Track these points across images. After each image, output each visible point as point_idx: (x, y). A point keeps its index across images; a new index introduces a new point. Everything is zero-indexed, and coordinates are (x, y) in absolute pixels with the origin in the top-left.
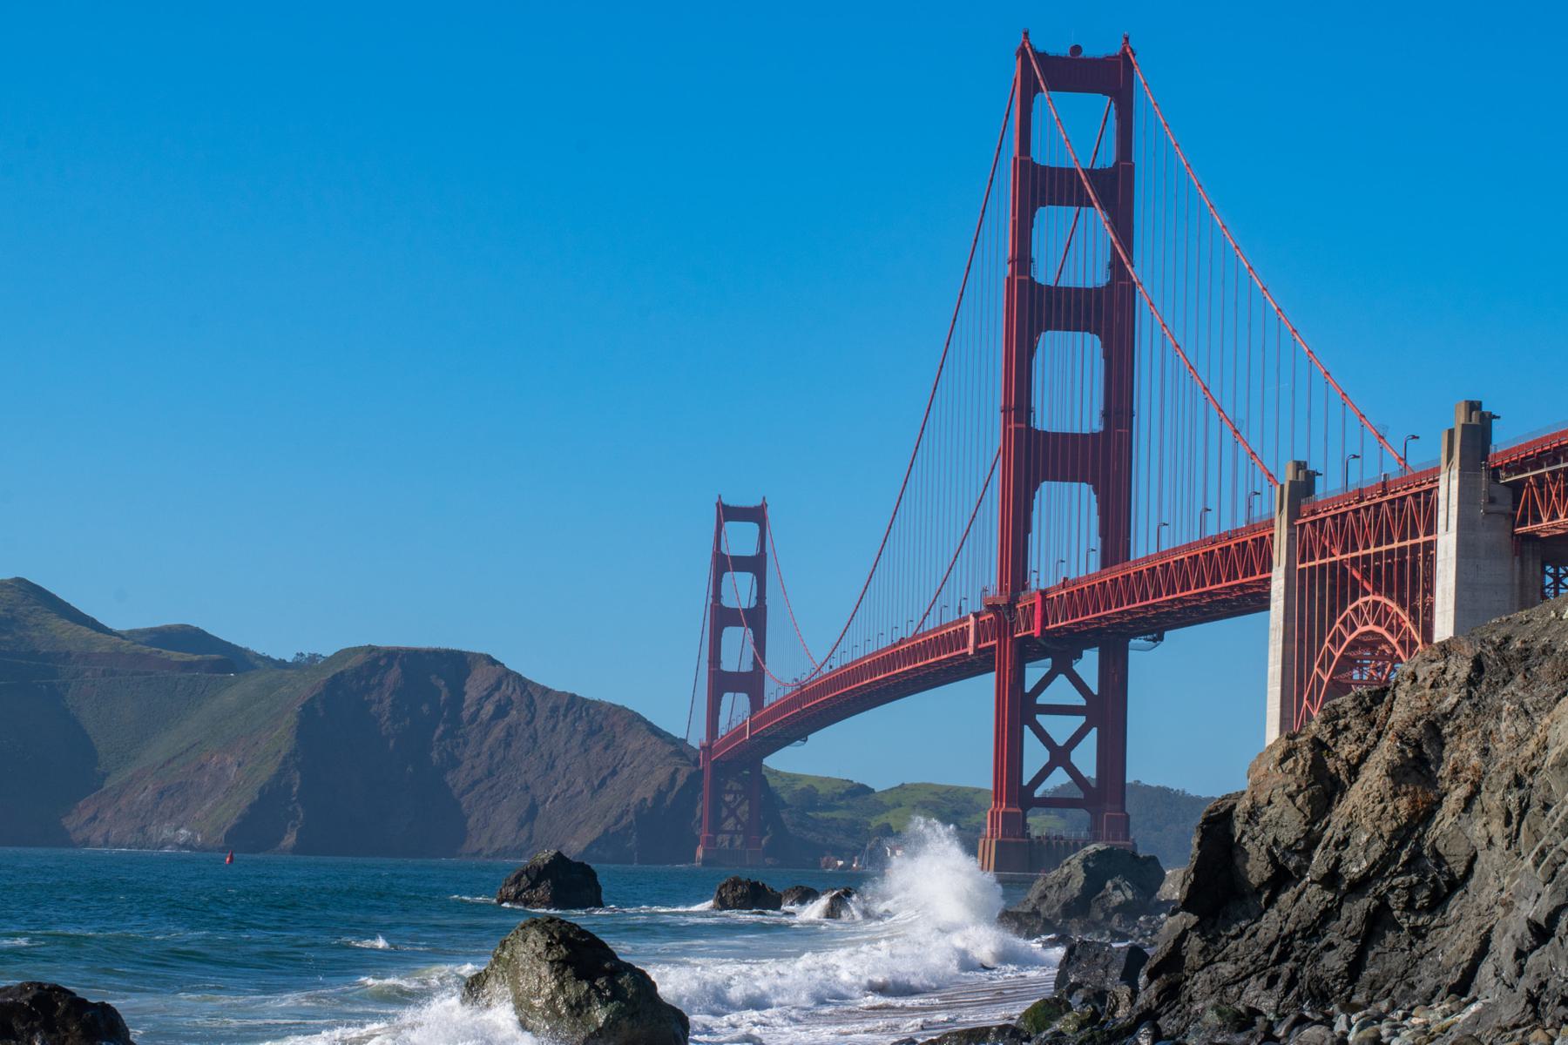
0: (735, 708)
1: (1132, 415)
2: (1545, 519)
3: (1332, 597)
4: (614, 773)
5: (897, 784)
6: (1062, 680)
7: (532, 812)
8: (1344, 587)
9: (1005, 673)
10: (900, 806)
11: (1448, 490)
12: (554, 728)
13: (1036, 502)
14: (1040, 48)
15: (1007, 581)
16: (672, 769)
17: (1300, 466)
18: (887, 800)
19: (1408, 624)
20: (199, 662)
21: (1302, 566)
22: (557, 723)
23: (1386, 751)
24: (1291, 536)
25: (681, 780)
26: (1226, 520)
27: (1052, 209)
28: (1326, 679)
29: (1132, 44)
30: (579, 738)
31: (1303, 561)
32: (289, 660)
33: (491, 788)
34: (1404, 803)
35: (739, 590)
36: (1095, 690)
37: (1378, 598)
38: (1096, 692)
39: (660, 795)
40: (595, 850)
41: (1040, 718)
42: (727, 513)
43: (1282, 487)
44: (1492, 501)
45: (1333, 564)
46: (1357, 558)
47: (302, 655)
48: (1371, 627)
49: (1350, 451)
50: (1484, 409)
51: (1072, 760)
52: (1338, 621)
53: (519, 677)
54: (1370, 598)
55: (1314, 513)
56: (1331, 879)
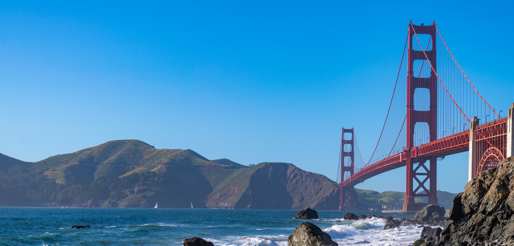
0: (347, 175)
1: (437, 107)
3: (483, 147)
4: (321, 190)
6: (421, 167)
7: (302, 199)
8: (486, 145)
9: (408, 166)
10: (385, 196)
12: (307, 180)
13: (415, 127)
14: (414, 24)
15: (408, 145)
16: (333, 189)
17: (475, 118)
18: (382, 195)
19: (501, 154)
20: (228, 167)
21: (476, 141)
22: (308, 179)
23: (496, 182)
24: (473, 134)
25: (335, 191)
26: (459, 130)
27: (417, 60)
28: (482, 166)
30: (312, 182)
31: (476, 139)
32: (248, 166)
33: (293, 193)
34: (500, 194)
35: (348, 148)
36: (429, 169)
37: (493, 148)
39: (331, 194)
40: (316, 207)
41: (417, 176)
42: (345, 131)
43: (471, 122)
45: (483, 140)
46: (489, 139)
47: (251, 165)
48: (492, 154)
49: (487, 114)
51: (424, 186)
52: (485, 153)
53: (299, 168)
54: (492, 148)
55: (479, 128)
56: (484, 212)
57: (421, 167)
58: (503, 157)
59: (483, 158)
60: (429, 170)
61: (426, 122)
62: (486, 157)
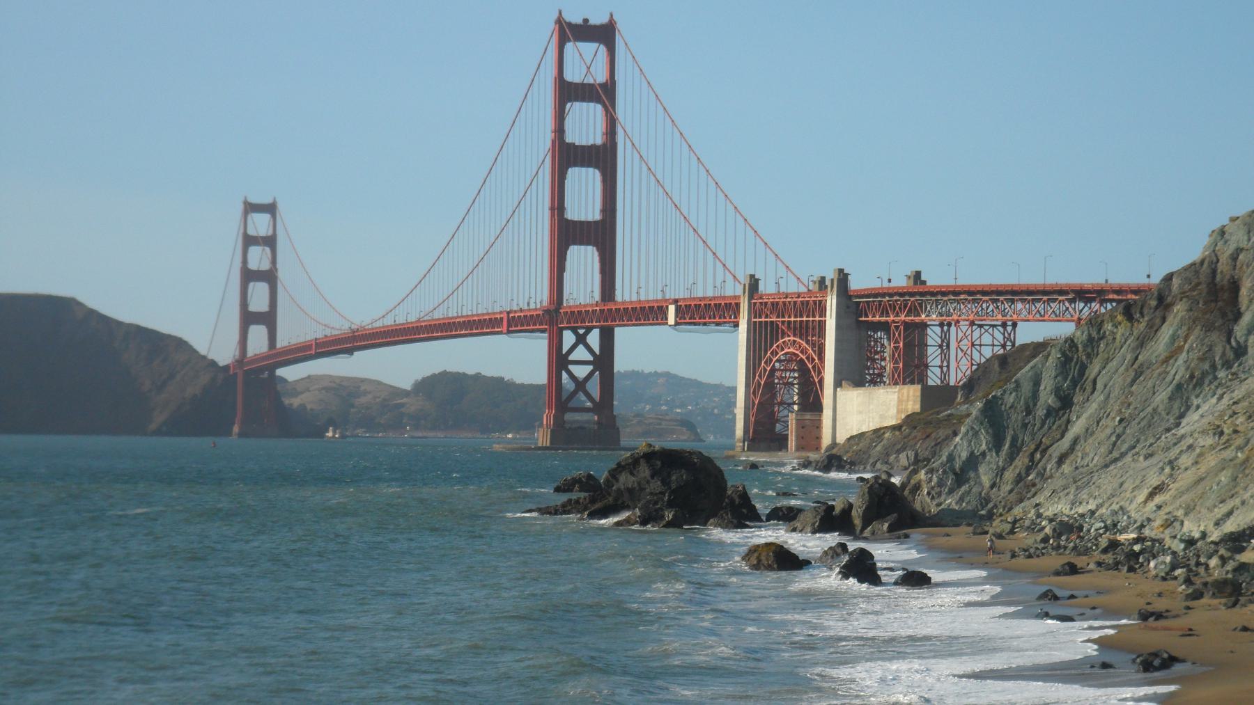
2: (870, 317)
5: (305, 375)
6: (581, 347)
8: (777, 331)
11: (831, 302)
19: (811, 351)
21: (755, 320)
29: (615, 18)
31: (755, 317)
35: (258, 258)
36: (597, 351)
38: (598, 353)
42: (251, 208)
44: (848, 307)
45: (772, 322)
46: (785, 321)
48: (792, 350)
49: (778, 276)
50: (845, 272)
55: (761, 298)
57: (581, 347)
58: (816, 359)
61: (588, 244)
62: (777, 353)
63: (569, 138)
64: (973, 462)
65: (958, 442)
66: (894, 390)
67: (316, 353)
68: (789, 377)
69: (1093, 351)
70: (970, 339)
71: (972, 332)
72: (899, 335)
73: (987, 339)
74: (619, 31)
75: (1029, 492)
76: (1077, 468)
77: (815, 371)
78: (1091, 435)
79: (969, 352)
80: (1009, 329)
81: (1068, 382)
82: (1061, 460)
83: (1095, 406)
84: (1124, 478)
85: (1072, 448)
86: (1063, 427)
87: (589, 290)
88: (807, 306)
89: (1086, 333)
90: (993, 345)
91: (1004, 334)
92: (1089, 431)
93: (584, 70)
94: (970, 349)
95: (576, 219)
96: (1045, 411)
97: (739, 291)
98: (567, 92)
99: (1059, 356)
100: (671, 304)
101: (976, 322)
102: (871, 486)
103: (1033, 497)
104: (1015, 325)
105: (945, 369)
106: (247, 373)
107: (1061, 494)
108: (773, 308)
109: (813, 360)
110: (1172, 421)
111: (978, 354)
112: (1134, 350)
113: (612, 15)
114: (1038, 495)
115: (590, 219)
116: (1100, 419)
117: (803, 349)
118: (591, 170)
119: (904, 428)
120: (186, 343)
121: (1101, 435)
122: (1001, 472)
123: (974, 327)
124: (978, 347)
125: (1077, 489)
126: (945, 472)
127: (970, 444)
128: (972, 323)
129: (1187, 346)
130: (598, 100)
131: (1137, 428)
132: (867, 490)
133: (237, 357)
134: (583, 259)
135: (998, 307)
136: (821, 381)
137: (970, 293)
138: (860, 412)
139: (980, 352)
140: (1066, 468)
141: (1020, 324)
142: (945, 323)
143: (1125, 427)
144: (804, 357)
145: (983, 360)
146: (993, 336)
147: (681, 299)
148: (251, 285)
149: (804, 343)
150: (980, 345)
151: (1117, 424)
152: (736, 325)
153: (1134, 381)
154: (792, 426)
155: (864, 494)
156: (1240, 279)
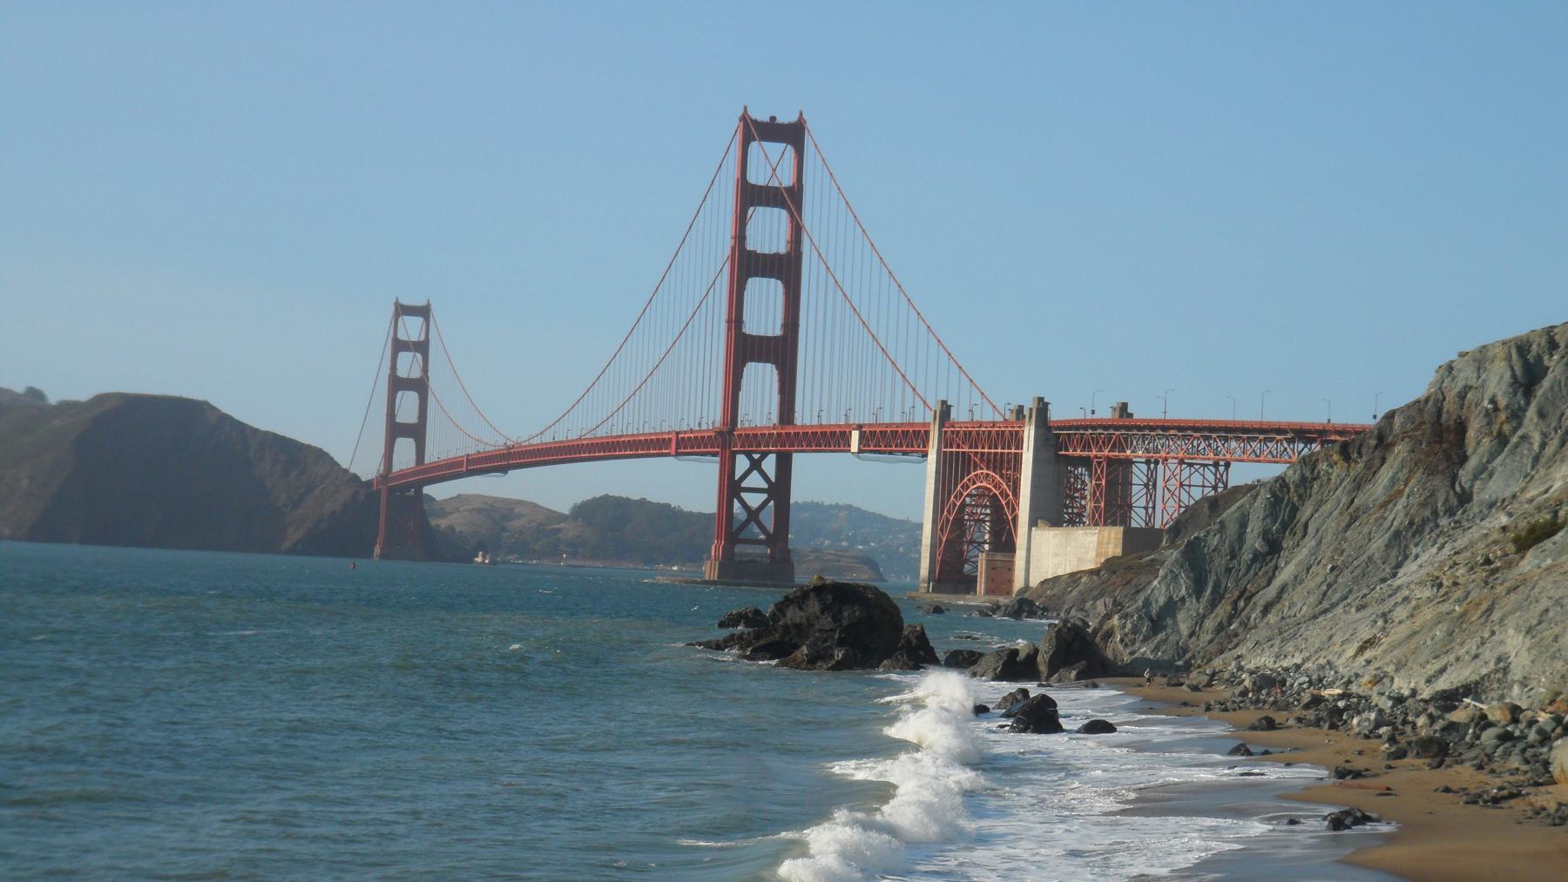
5: (455, 495)
6: (755, 473)
11: (1029, 434)
24: (940, 435)
31: (946, 447)
35: (408, 365)
36: (773, 480)
42: (402, 310)
44: (1048, 440)
48: (984, 484)
49: (972, 403)
55: (953, 426)
57: (755, 473)
58: (1011, 494)
59: (961, 487)
60: (773, 481)
61: (767, 361)
62: (968, 487)
63: (750, 246)
64: (1171, 607)
65: (1155, 587)
66: (1094, 532)
67: (467, 470)
68: (981, 514)
69: (1306, 492)
70: (1178, 479)
71: (1181, 471)
72: (1102, 471)
73: (1197, 479)
74: (809, 131)
75: (1231, 642)
76: (1283, 618)
77: (1008, 508)
78: (1300, 583)
79: (1177, 493)
80: (1222, 469)
81: (1277, 525)
82: (1266, 609)
83: (1305, 551)
84: (1334, 631)
85: (1279, 596)
86: (1270, 574)
87: (766, 411)
88: (1002, 437)
89: (1299, 472)
90: (1203, 486)
91: (1215, 475)
92: (1298, 578)
93: (770, 172)
94: (1178, 490)
95: (754, 334)
96: (1251, 556)
97: (929, 418)
98: (751, 196)
99: (1268, 496)
100: (854, 429)
101: (1186, 461)
102: (1060, 630)
103: (1235, 648)
104: (1227, 465)
105: (1150, 511)
106: (392, 490)
107: (1265, 646)
108: (966, 438)
109: (1008, 495)
110: (1388, 570)
111: (1187, 496)
112: (1350, 492)
113: (801, 114)
114: (1241, 646)
115: (770, 334)
116: (1311, 566)
117: (996, 484)
118: (773, 280)
119: (1102, 573)
120: (326, 454)
121: (1311, 583)
122: (1201, 619)
123: (1184, 466)
124: (1187, 488)
125: (1282, 641)
126: (1140, 618)
127: (1168, 589)
128: (1181, 462)
129: (1407, 489)
130: (783, 205)
131: (1350, 576)
132: (1054, 634)
133: (381, 472)
134: (761, 378)
135: (1210, 445)
136: (1015, 519)
137: (1180, 429)
138: (1056, 555)
139: (1189, 493)
140: (1272, 618)
141: (1233, 464)
142: (1153, 460)
143: (1337, 576)
144: (997, 493)
145: (1192, 502)
146: (1203, 476)
147: (866, 425)
148: (400, 394)
149: (997, 477)
150: (1190, 486)
151: (1328, 571)
152: (925, 455)
153: (1348, 526)
154: (981, 568)
155: (1051, 639)
156: (1467, 420)
